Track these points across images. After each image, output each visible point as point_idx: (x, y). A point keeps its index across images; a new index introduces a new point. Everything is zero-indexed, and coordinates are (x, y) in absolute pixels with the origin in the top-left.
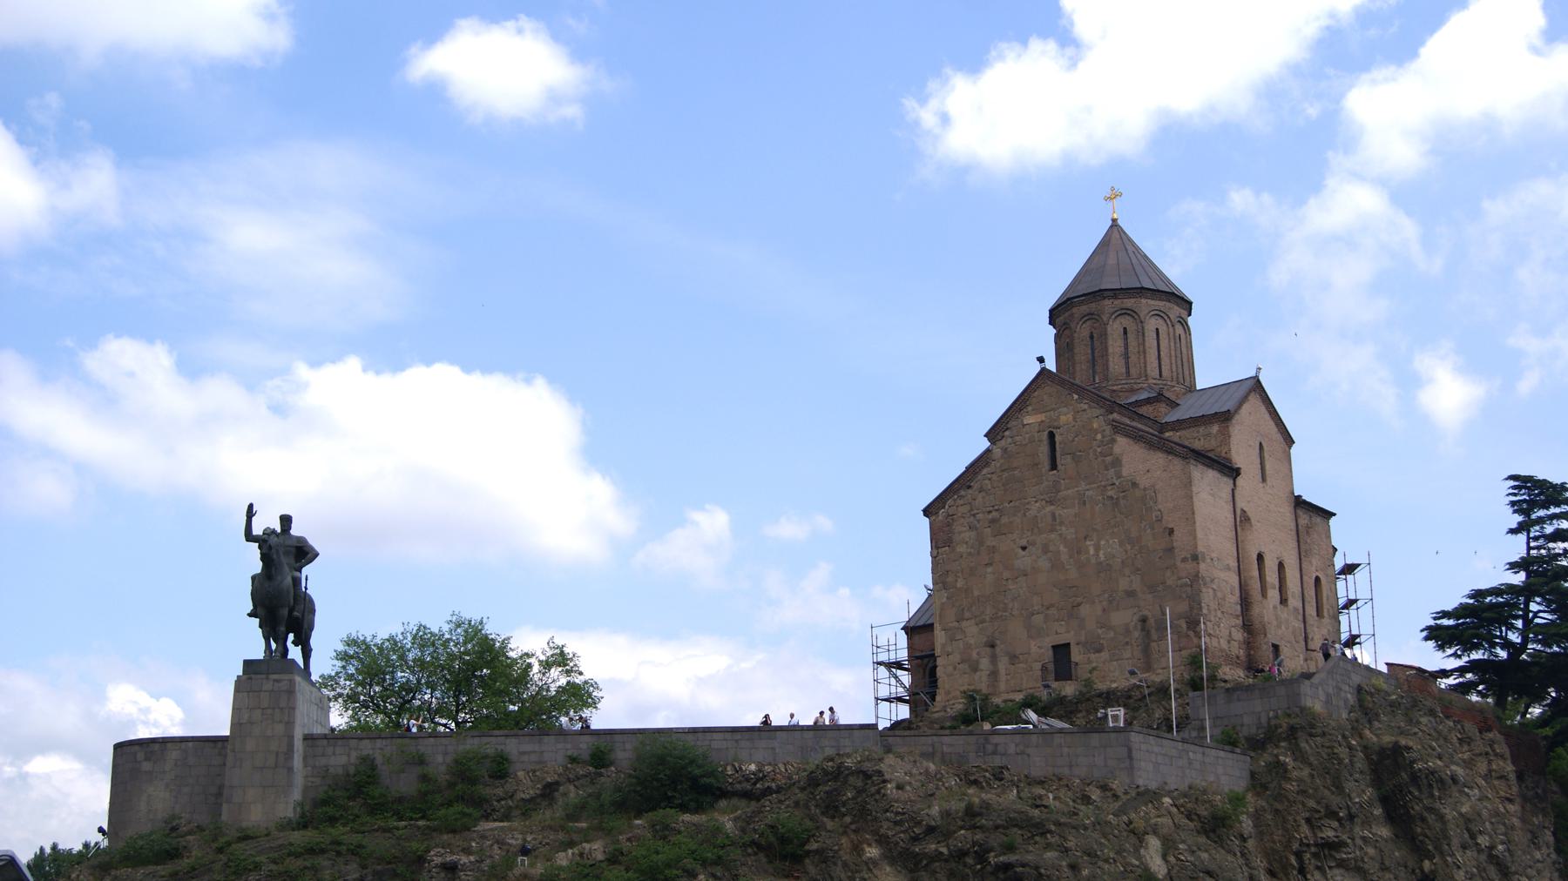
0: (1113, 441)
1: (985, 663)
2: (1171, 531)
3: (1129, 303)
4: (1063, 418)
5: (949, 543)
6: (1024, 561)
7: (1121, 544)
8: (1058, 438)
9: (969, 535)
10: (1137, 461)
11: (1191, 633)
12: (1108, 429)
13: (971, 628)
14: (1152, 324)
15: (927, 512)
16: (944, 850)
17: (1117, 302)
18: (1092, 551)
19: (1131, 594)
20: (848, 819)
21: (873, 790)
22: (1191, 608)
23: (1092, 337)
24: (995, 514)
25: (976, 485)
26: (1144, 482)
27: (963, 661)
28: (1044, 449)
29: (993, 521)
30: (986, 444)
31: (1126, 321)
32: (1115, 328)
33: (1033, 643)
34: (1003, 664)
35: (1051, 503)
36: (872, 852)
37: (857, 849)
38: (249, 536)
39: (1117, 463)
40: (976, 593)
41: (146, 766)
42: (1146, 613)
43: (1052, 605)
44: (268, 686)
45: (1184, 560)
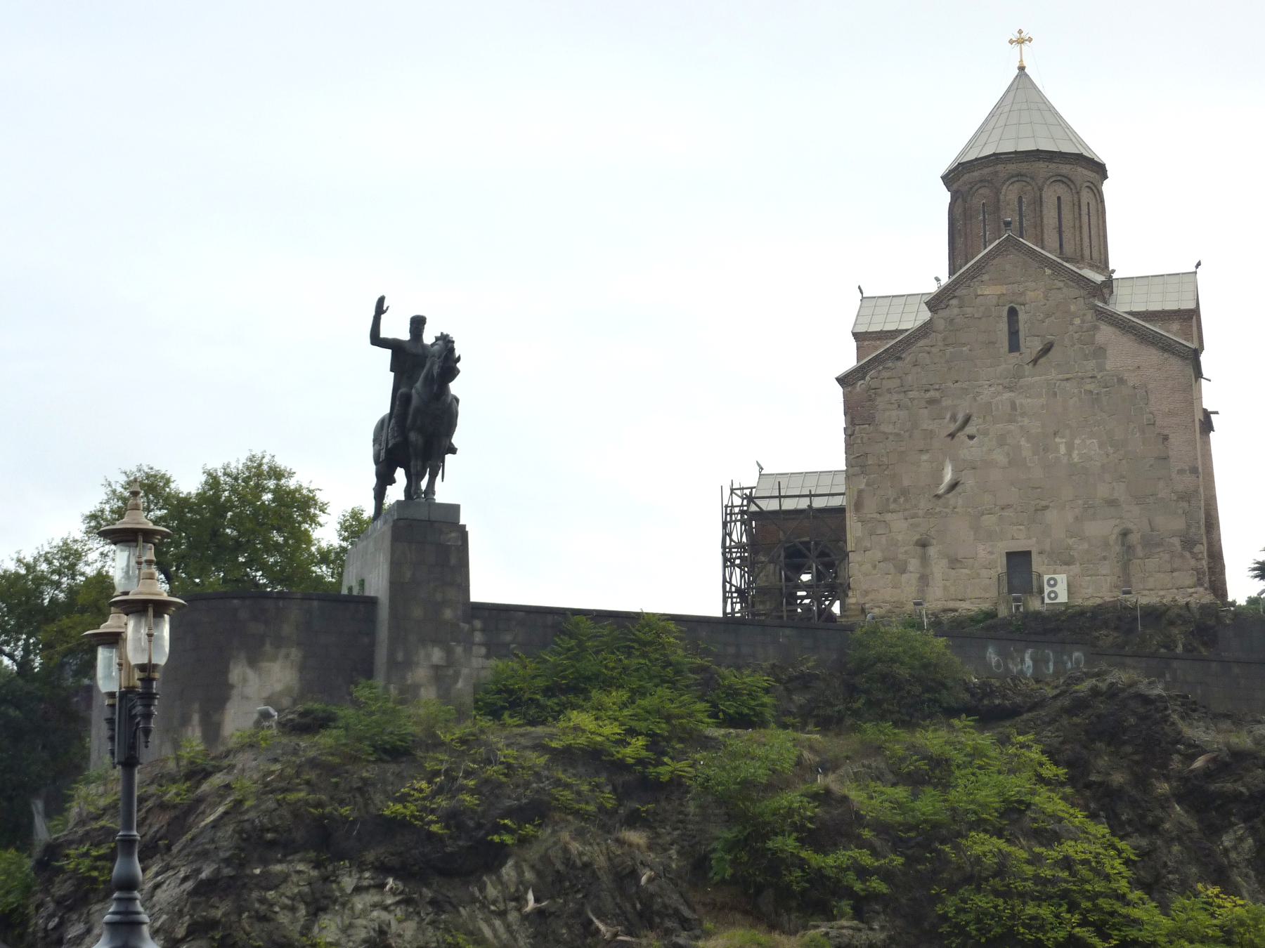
0: (1096, 328)
1: (914, 564)
2: (1166, 438)
3: (1065, 169)
4: (1030, 294)
5: (870, 420)
7: (1101, 445)
8: (1022, 317)
10: (1122, 354)
11: (1187, 554)
12: (1090, 315)
13: (898, 524)
15: (840, 380)
16: (1243, 790)
17: (1052, 166)
18: (1063, 450)
19: (1113, 503)
20: (1129, 749)
21: (1158, 716)
22: (1189, 526)
24: (932, 394)
25: (908, 358)
26: (1132, 380)
27: (885, 560)
28: (1003, 326)
29: (932, 402)
30: (926, 315)
31: (1061, 190)
32: (1050, 196)
33: (981, 548)
34: (939, 568)
35: (1011, 389)
38: (376, 340)
39: (1100, 352)
40: (906, 483)
42: (1131, 526)
43: (1009, 506)
45: (1181, 472)
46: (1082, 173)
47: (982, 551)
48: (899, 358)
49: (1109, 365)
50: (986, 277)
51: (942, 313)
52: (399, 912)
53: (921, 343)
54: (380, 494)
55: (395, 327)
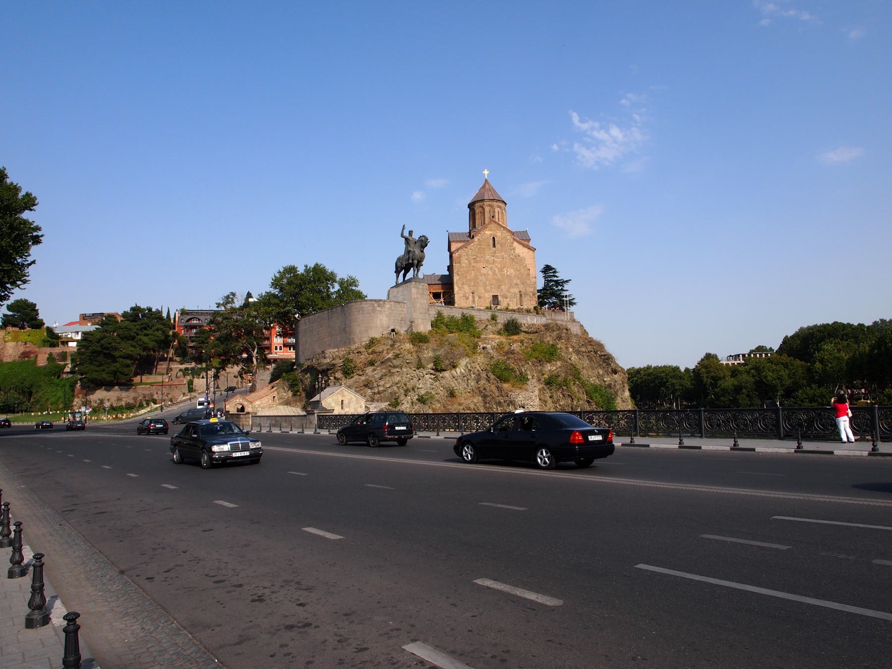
1: (471, 298)
6: (484, 271)
9: (466, 261)
10: (520, 250)
13: (466, 288)
14: (497, 210)
26: (521, 255)
28: (491, 241)
34: (476, 298)
36: (571, 350)
37: (567, 348)
38: (402, 236)
39: (514, 249)
41: (378, 309)
46: (502, 205)
47: (487, 295)
49: (517, 252)
54: (398, 277)
55: (406, 234)
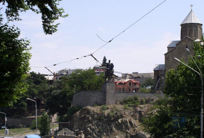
4: (189, 44)
5: (168, 60)
17: (194, 25)
23: (190, 30)
31: (195, 28)
35: (186, 56)
41: (93, 95)
44: (111, 85)
48: (172, 52)
50: (183, 42)
51: (178, 46)
52: (108, 125)
53: (175, 50)
